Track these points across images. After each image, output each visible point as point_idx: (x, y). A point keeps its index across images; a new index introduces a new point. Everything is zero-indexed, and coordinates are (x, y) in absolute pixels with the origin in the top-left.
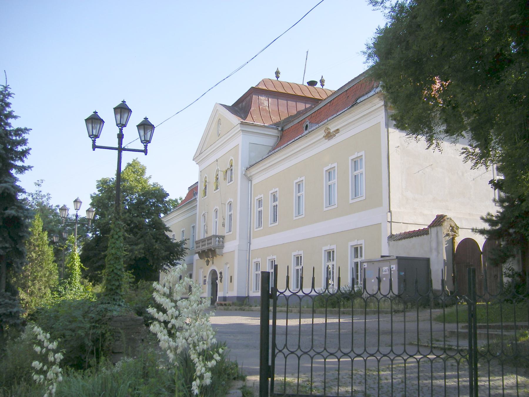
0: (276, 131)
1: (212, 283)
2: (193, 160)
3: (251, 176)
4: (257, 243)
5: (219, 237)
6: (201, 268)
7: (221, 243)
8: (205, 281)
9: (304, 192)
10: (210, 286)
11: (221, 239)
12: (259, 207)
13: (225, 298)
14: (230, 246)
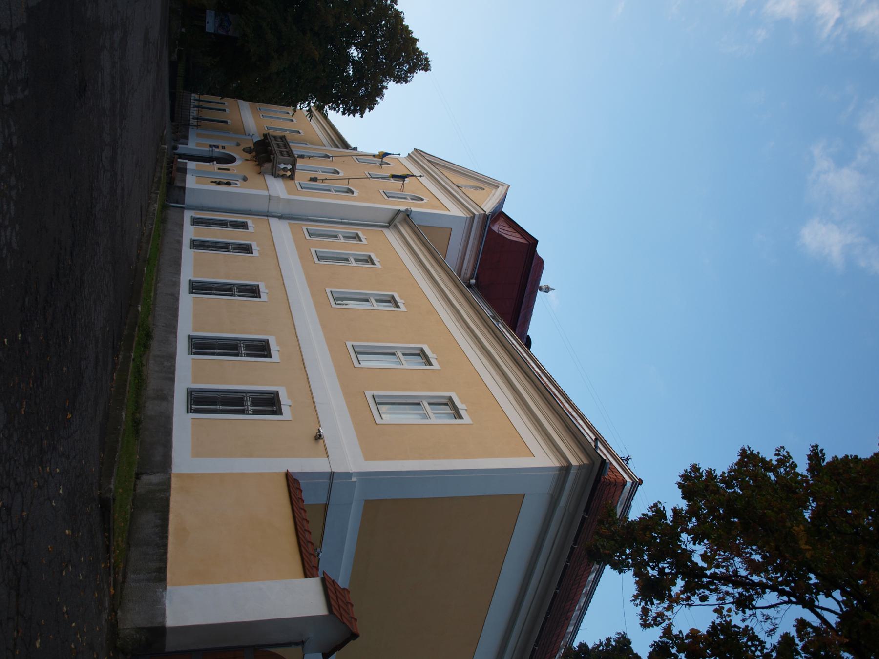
0: (468, 276)
3: (396, 226)
4: (281, 230)
5: (293, 171)
6: (238, 145)
7: (282, 173)
8: (217, 147)
9: (376, 308)
11: (289, 173)
13: (184, 171)
14: (277, 187)
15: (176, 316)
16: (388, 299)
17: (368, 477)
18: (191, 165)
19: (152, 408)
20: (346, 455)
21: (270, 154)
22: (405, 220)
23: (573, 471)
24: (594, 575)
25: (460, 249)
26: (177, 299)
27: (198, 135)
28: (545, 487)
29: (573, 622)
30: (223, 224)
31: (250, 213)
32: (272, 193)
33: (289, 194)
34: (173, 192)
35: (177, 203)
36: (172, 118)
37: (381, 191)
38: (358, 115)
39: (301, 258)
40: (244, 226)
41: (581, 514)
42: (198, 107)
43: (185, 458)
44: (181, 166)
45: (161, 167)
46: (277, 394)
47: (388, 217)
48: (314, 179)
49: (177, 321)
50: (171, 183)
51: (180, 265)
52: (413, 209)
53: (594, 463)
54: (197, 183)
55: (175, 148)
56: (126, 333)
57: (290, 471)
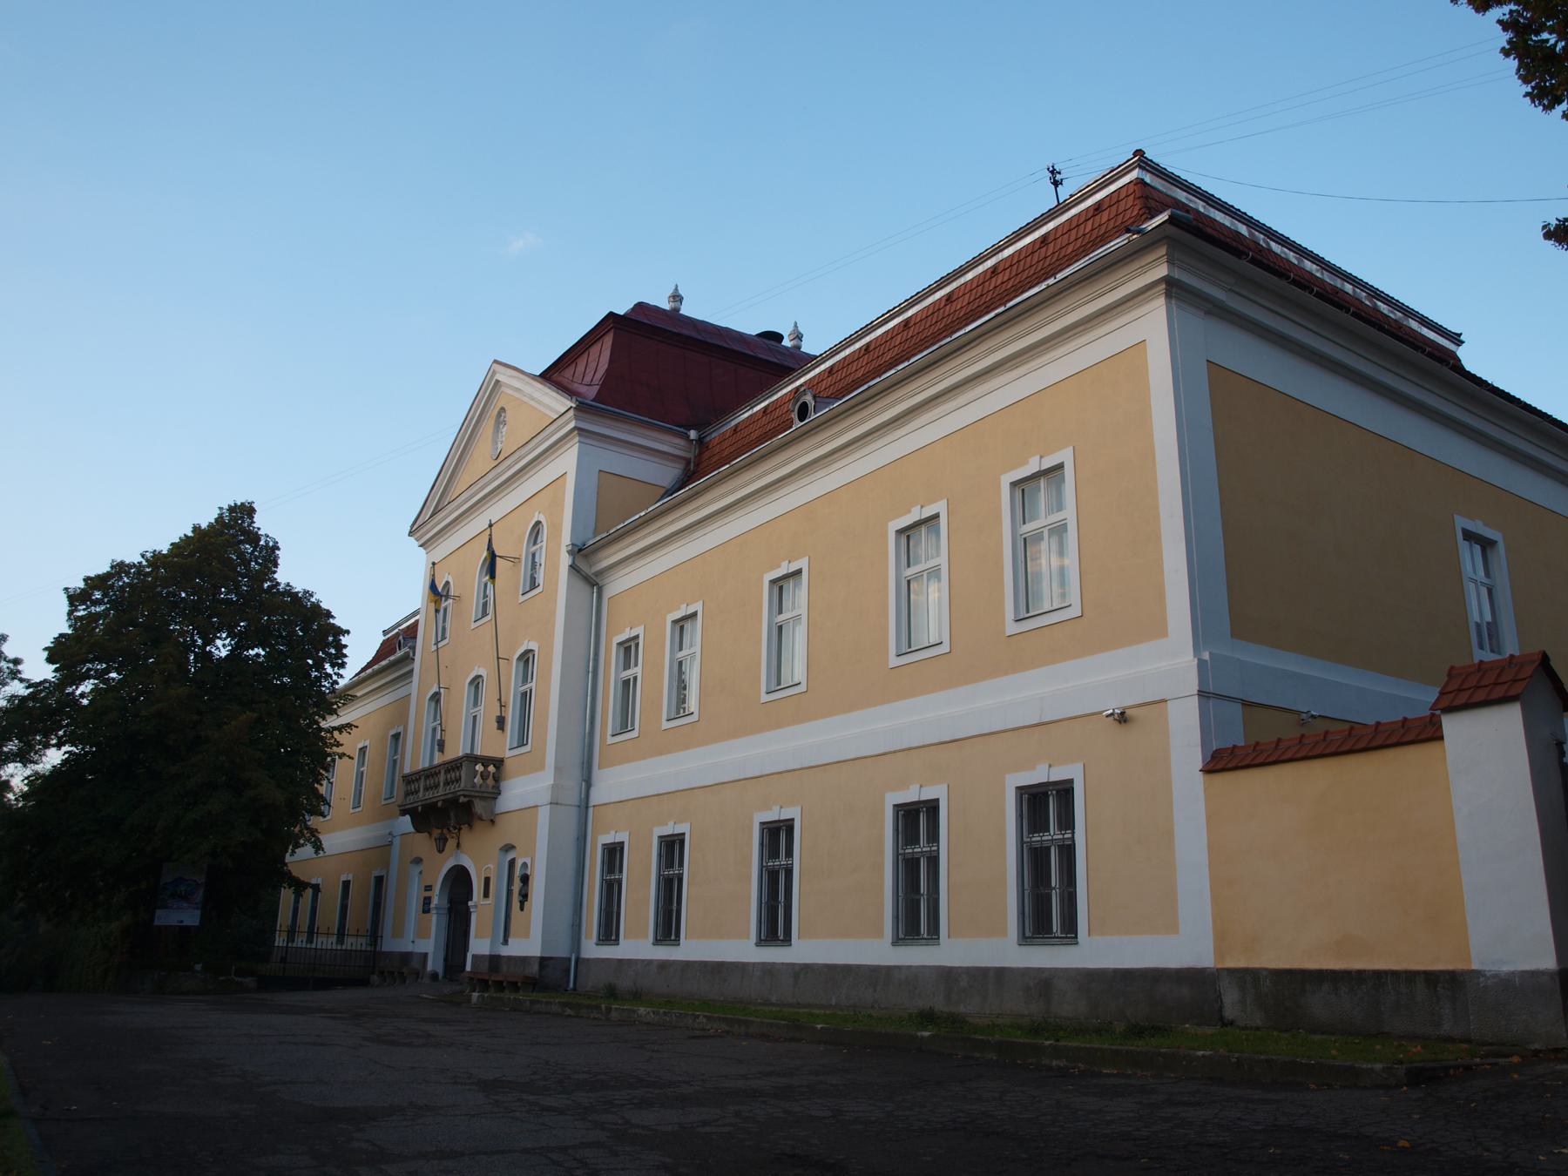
0: (682, 442)
1: (450, 910)
2: (411, 533)
5: (486, 761)
6: (418, 861)
7: (490, 781)
8: (427, 901)
10: (445, 920)
11: (491, 769)
12: (627, 666)
14: (528, 790)
15: (847, 969)
16: (776, 590)
17: (1200, 636)
18: (479, 945)
19: (1069, 1007)
20: (1165, 666)
21: (450, 802)
22: (586, 556)
23: (1177, 274)
24: (1273, 245)
25: (646, 458)
26: (807, 968)
27: (399, 932)
28: (1199, 325)
29: (1338, 283)
30: (611, 891)
31: (582, 839)
32: (546, 797)
33: (542, 767)
34: (548, 979)
35: (568, 970)
36: (364, 982)
37: (522, 599)
38: (344, 640)
39: (686, 748)
40: (614, 853)
41: (1244, 265)
42: (311, 933)
43: (1187, 945)
44: (485, 967)
45: (532, 1002)
46: (1021, 790)
47: (581, 586)
48: (501, 722)
49: (859, 967)
50: (534, 984)
51: (721, 964)
52: (566, 539)
53: (1166, 237)
54: (527, 935)
55: (434, 976)
56: (993, 1056)
57: (1200, 765)
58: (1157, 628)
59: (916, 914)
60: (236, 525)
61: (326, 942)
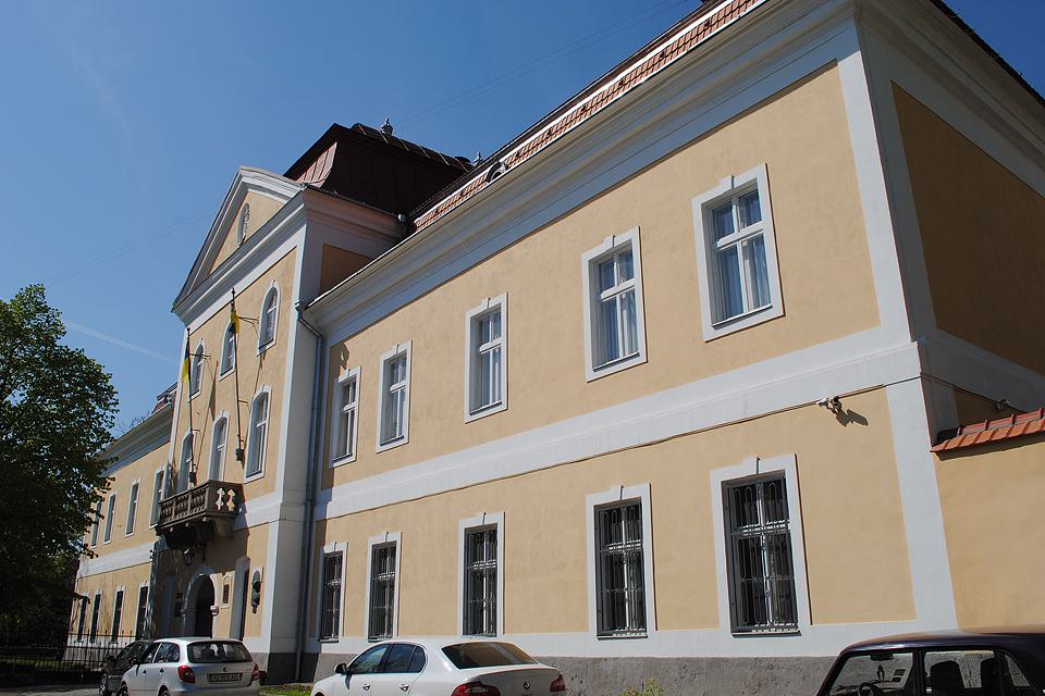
5: (226, 487)
7: (231, 505)
11: (231, 493)
40: (334, 562)
48: (240, 455)
54: (258, 633)
58: (868, 317)
59: (619, 607)
60: (33, 301)
61: (102, 642)
